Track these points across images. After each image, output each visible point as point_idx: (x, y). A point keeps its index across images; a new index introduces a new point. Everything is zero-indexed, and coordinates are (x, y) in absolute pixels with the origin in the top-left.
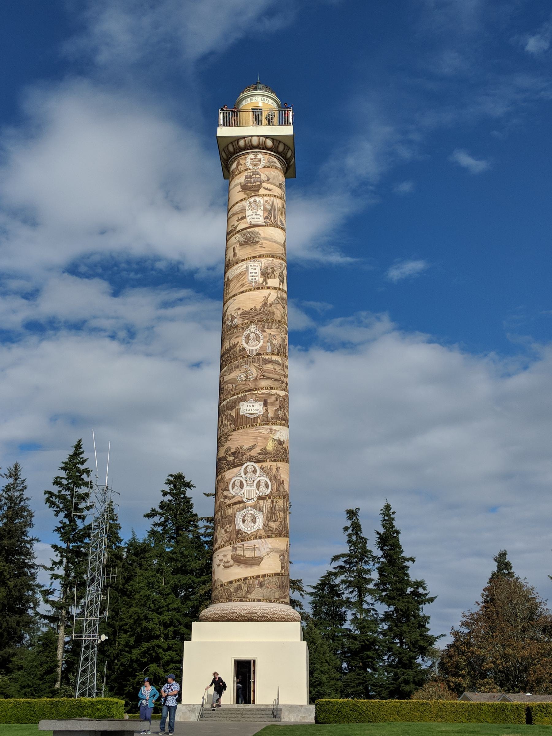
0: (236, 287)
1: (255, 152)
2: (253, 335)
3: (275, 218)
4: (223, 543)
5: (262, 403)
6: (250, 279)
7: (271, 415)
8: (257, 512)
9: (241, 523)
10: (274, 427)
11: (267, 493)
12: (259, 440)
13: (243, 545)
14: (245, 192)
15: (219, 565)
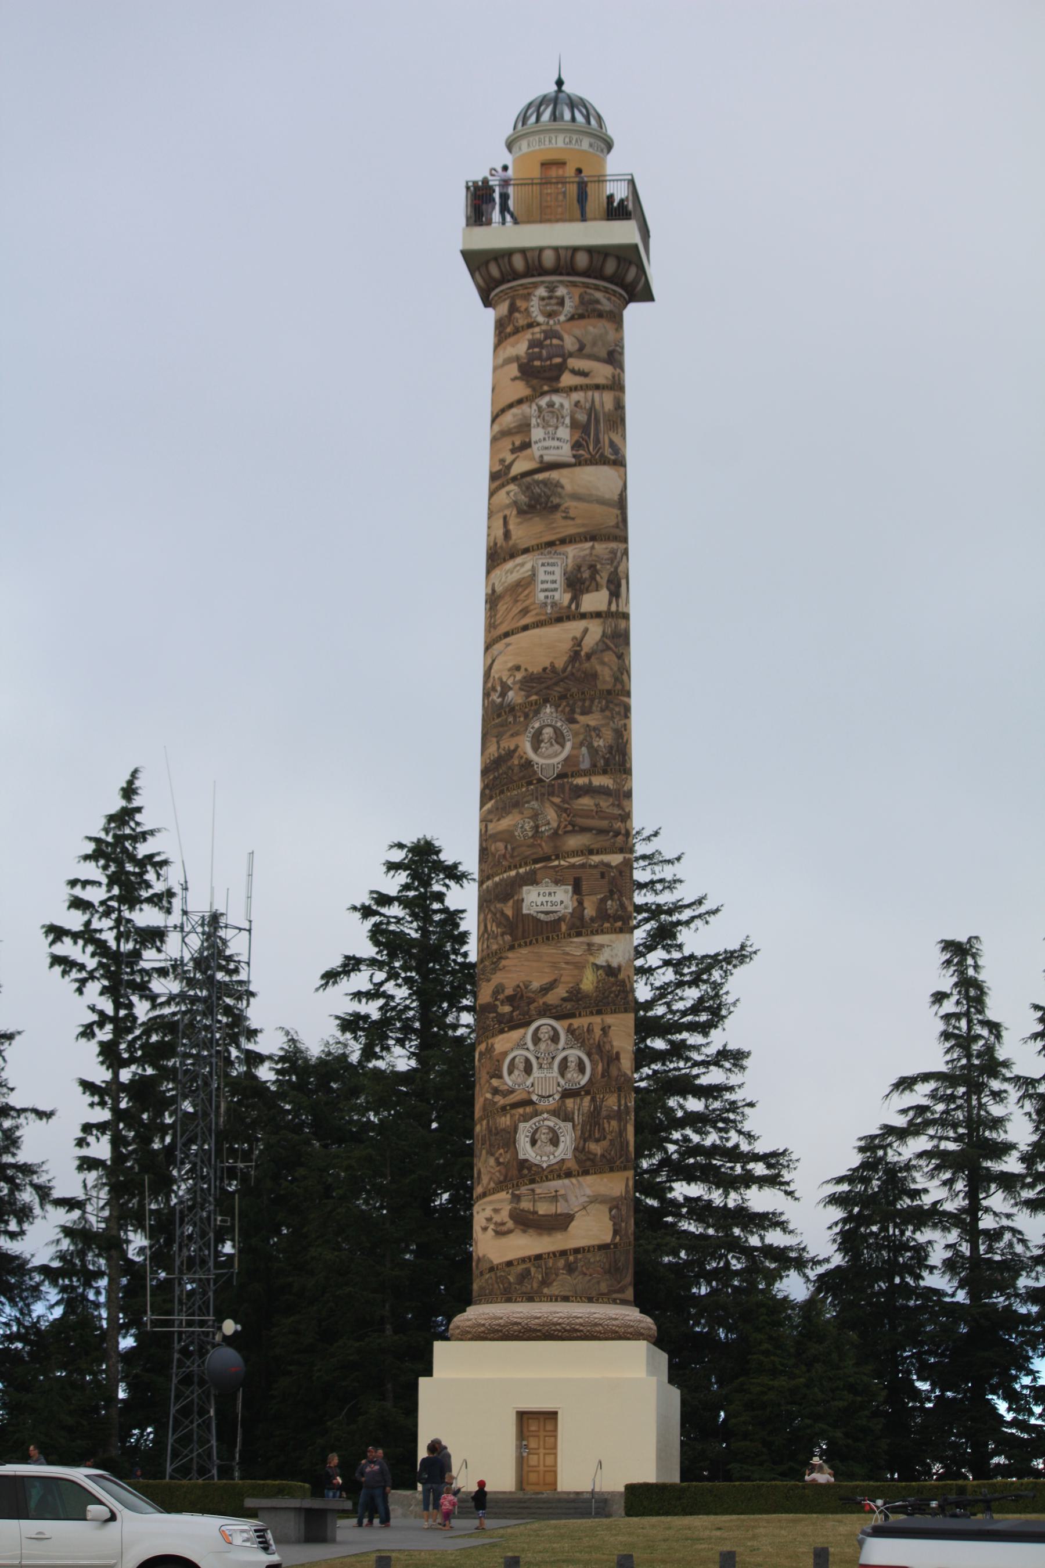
0: (512, 614)
1: (549, 282)
2: (548, 732)
3: (597, 441)
4: (492, 1185)
5: (570, 888)
6: (541, 596)
7: (589, 911)
8: (562, 1124)
9: (528, 1146)
10: (598, 939)
11: (583, 1083)
12: (564, 969)
13: (533, 1190)
14: (529, 384)
15: (485, 1229)
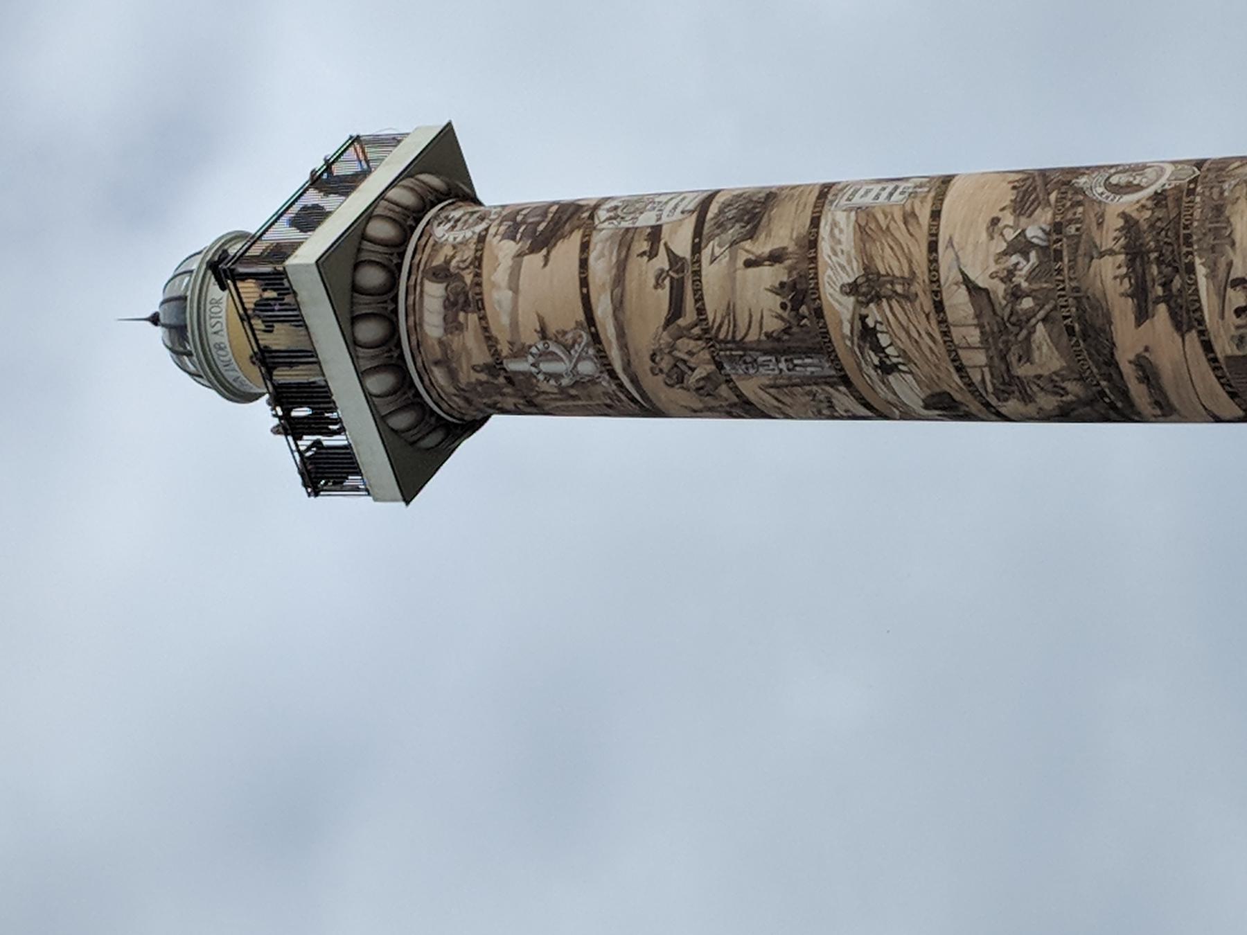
1: (436, 216)
14: (563, 237)
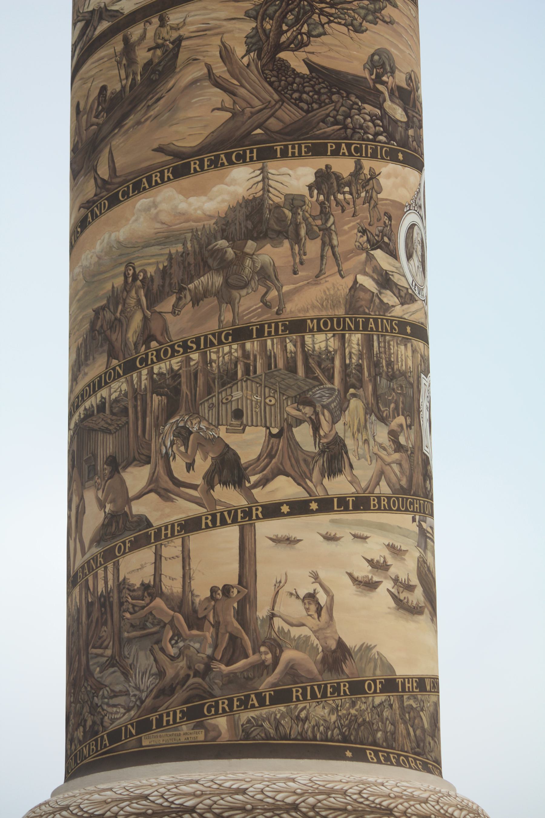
4: (384, 489)
